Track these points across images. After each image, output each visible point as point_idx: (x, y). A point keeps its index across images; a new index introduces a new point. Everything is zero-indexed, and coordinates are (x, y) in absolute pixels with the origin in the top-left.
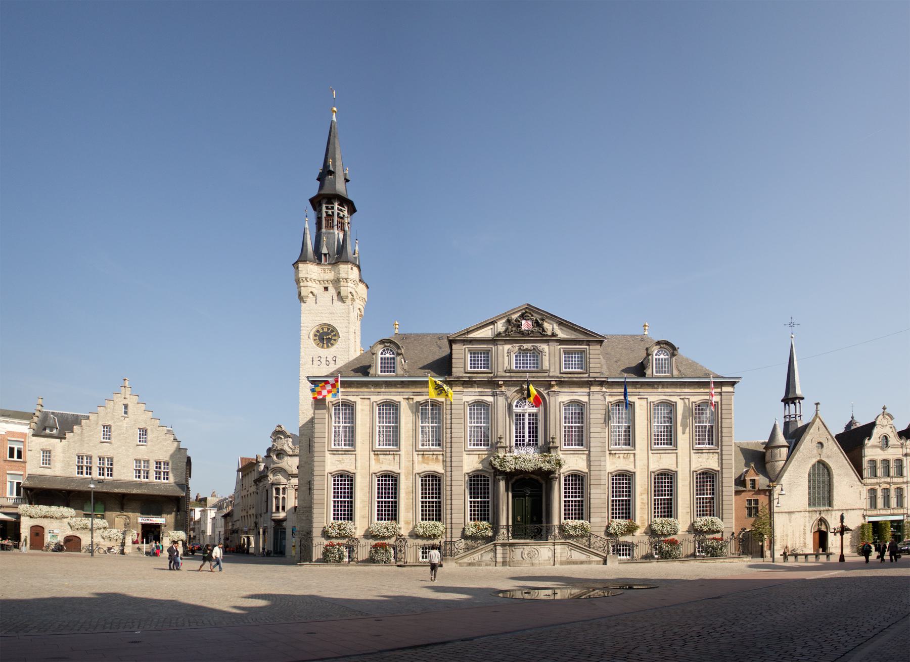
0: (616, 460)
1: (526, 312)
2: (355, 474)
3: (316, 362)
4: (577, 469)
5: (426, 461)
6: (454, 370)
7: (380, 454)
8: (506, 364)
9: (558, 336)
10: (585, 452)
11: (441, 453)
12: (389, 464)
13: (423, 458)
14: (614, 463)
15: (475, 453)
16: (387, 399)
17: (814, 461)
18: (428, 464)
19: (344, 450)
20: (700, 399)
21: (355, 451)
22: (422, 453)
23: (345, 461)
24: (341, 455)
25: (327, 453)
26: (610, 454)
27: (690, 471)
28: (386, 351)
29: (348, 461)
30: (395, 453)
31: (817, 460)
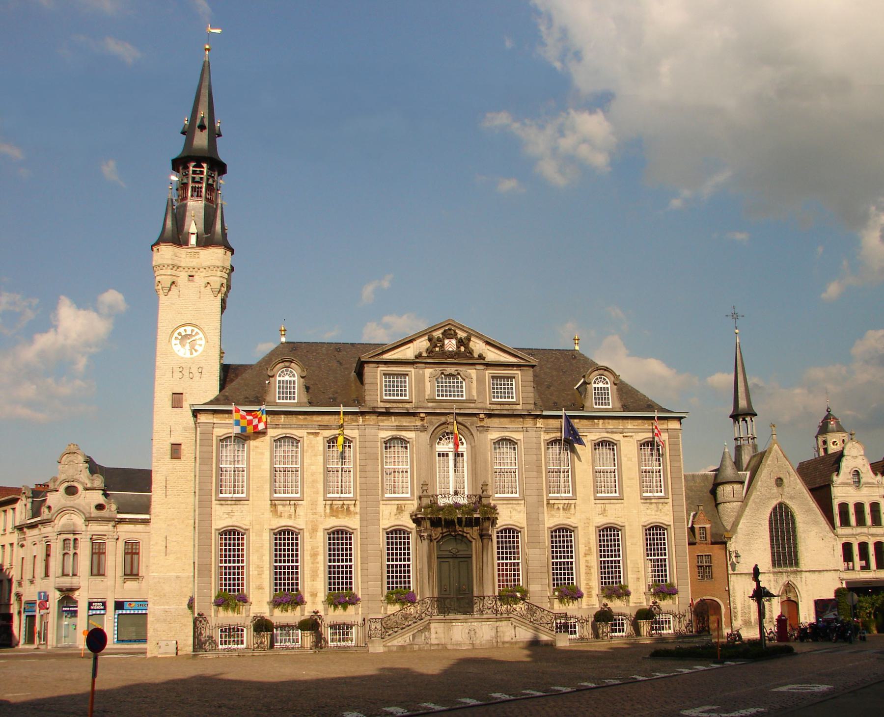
3: (177, 375)
4: (511, 523)
5: (335, 514)
6: (367, 398)
7: (279, 505)
8: (428, 391)
9: (486, 360)
10: (520, 502)
12: (290, 516)
14: (553, 516)
15: (393, 502)
16: (286, 434)
17: (774, 503)
18: (337, 517)
19: (234, 499)
20: (647, 437)
22: (330, 502)
23: (235, 514)
24: (229, 506)
25: (214, 502)
26: (548, 504)
28: (285, 373)
29: (239, 514)
30: (295, 502)
31: (778, 502)
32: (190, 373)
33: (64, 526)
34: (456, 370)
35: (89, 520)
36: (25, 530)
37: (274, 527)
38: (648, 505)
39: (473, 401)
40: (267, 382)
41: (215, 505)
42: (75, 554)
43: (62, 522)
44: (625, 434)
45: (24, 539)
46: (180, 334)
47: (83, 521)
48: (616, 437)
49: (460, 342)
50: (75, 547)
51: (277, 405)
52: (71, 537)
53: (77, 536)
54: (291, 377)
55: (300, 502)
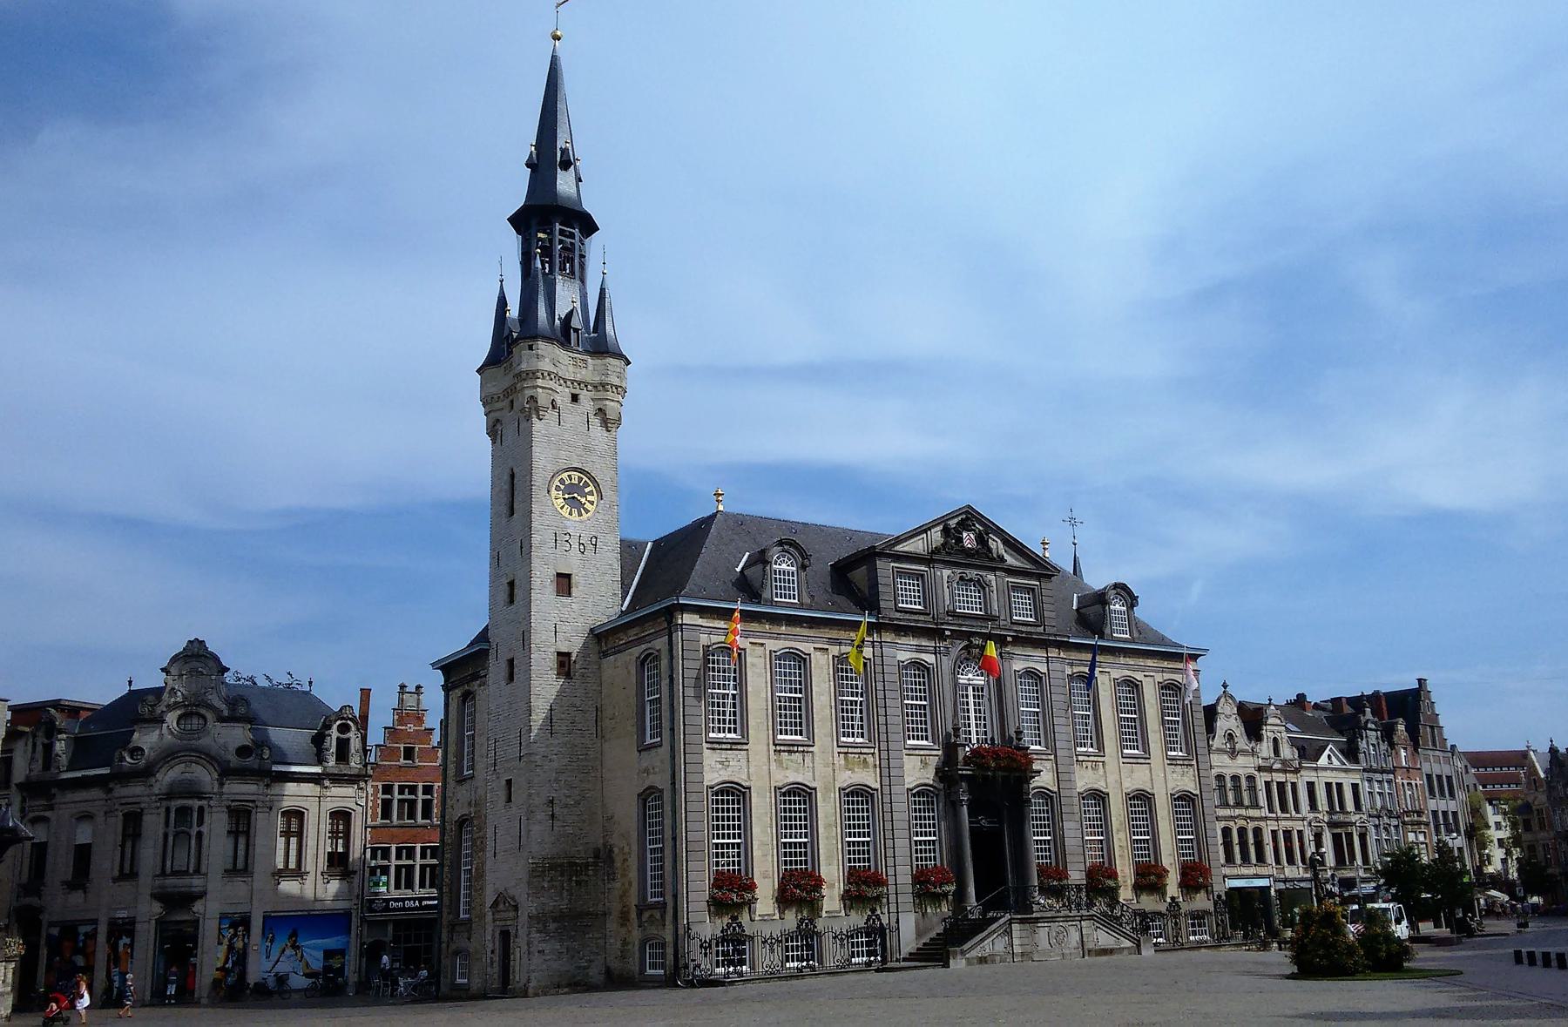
0: (1083, 772)
1: (967, 518)
2: (749, 788)
6: (882, 604)
7: (784, 751)
8: (947, 603)
10: (1050, 757)
11: (872, 751)
12: (797, 771)
13: (846, 759)
15: (917, 752)
18: (853, 771)
21: (747, 744)
27: (1167, 794)
30: (805, 748)
32: (580, 544)
33: (172, 784)
34: (977, 575)
35: (227, 772)
36: (54, 791)
37: (780, 784)
38: (1173, 766)
39: (993, 619)
40: (738, 569)
41: (707, 753)
42: (200, 834)
43: (168, 776)
44: (1145, 673)
45: (51, 808)
46: (562, 481)
47: (216, 776)
48: (1139, 676)
49: (981, 540)
50: (201, 822)
51: (772, 603)
52: (196, 803)
53: (204, 803)
54: (788, 566)
55: (811, 749)
